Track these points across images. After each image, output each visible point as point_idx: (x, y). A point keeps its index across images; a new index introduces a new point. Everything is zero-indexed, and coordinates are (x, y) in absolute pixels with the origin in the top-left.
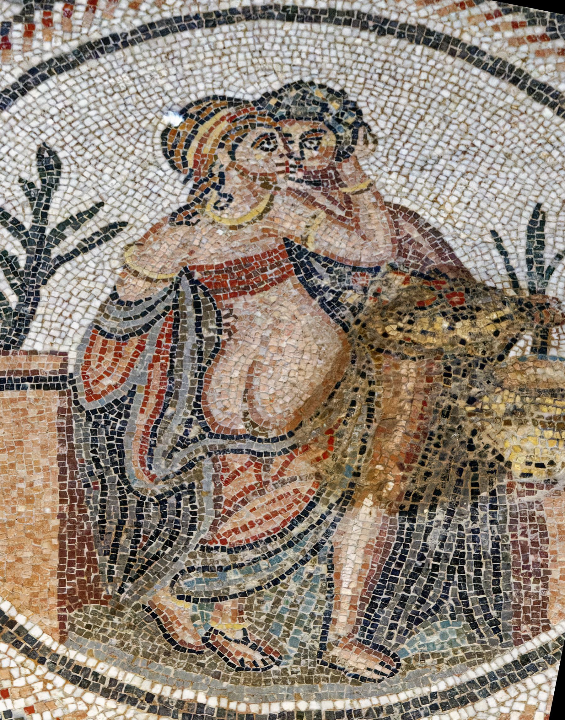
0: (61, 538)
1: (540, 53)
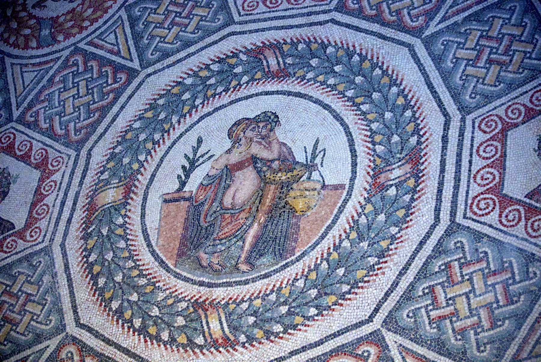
1: (328, 96)
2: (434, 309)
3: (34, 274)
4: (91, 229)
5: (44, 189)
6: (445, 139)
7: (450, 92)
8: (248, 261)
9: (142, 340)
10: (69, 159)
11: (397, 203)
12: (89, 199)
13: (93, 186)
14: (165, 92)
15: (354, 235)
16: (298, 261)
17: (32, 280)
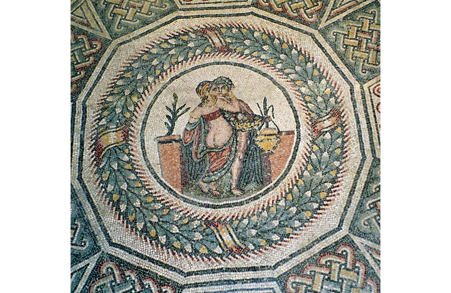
0: (181, 172)
1: (264, 67)
4: (102, 165)
6: (353, 101)
7: (348, 68)
8: (238, 187)
9: (171, 254)
11: (334, 144)
12: (94, 141)
13: (94, 130)
14: (137, 58)
15: (310, 167)
16: (276, 186)
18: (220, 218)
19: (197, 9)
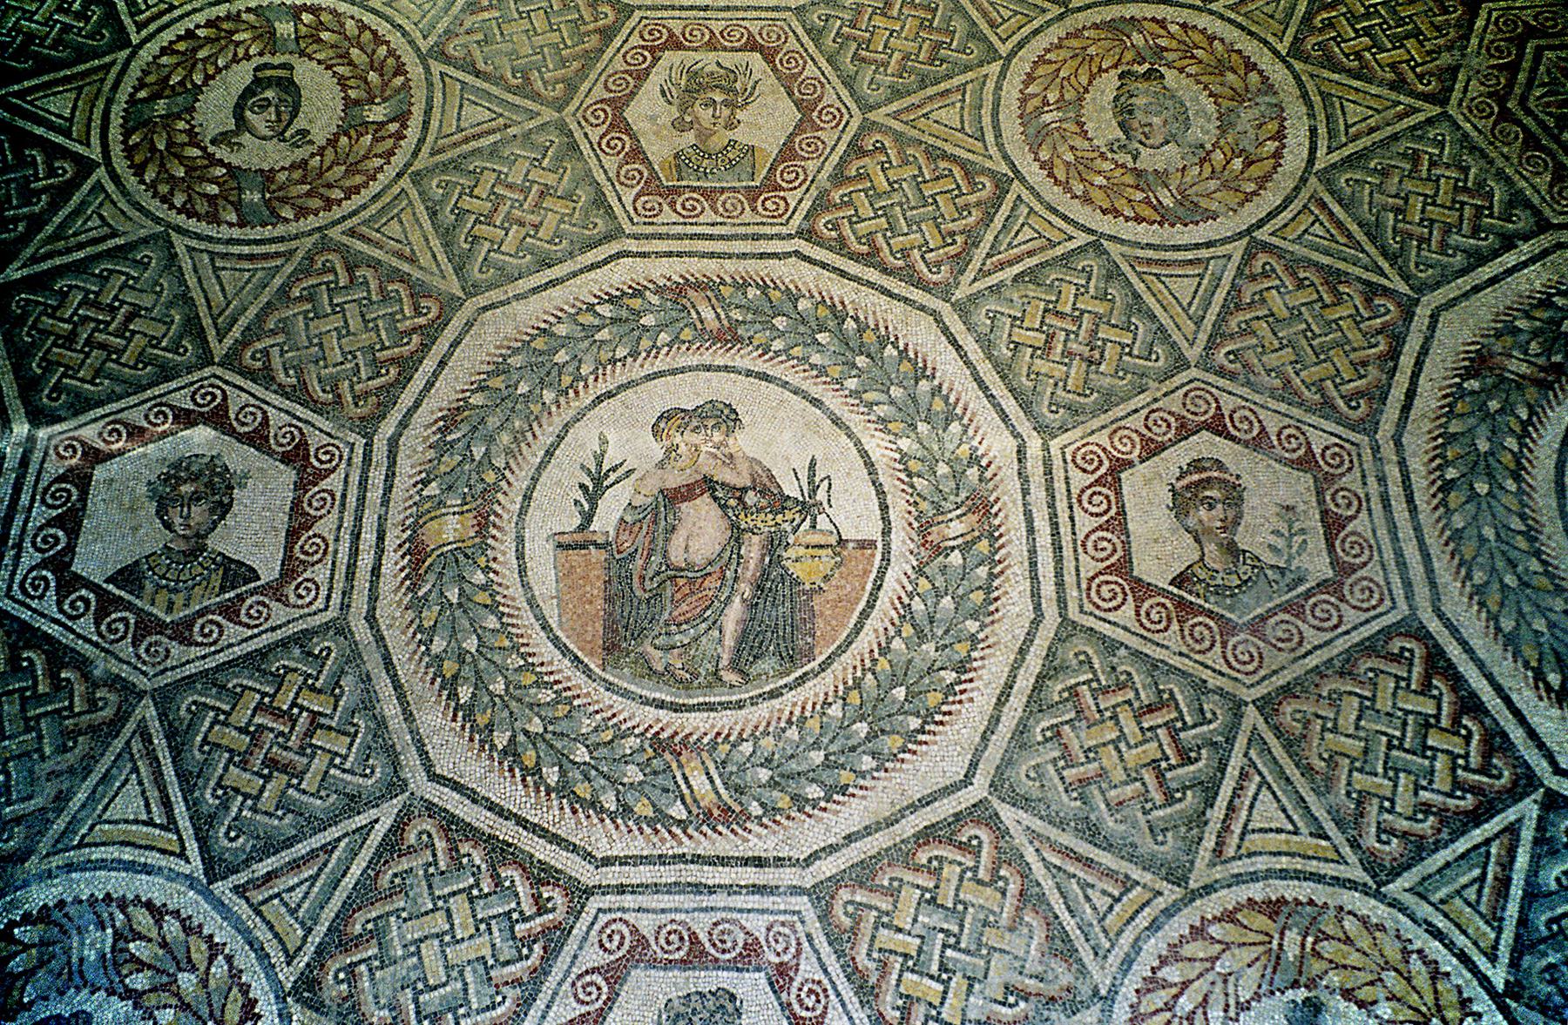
2: (1068, 766)
3: (320, 672)
4: (424, 590)
5: (310, 505)
8: (735, 666)
9: (567, 810)
10: (352, 450)
15: (908, 630)
17: (318, 685)
18: (687, 736)
19: (668, 237)
